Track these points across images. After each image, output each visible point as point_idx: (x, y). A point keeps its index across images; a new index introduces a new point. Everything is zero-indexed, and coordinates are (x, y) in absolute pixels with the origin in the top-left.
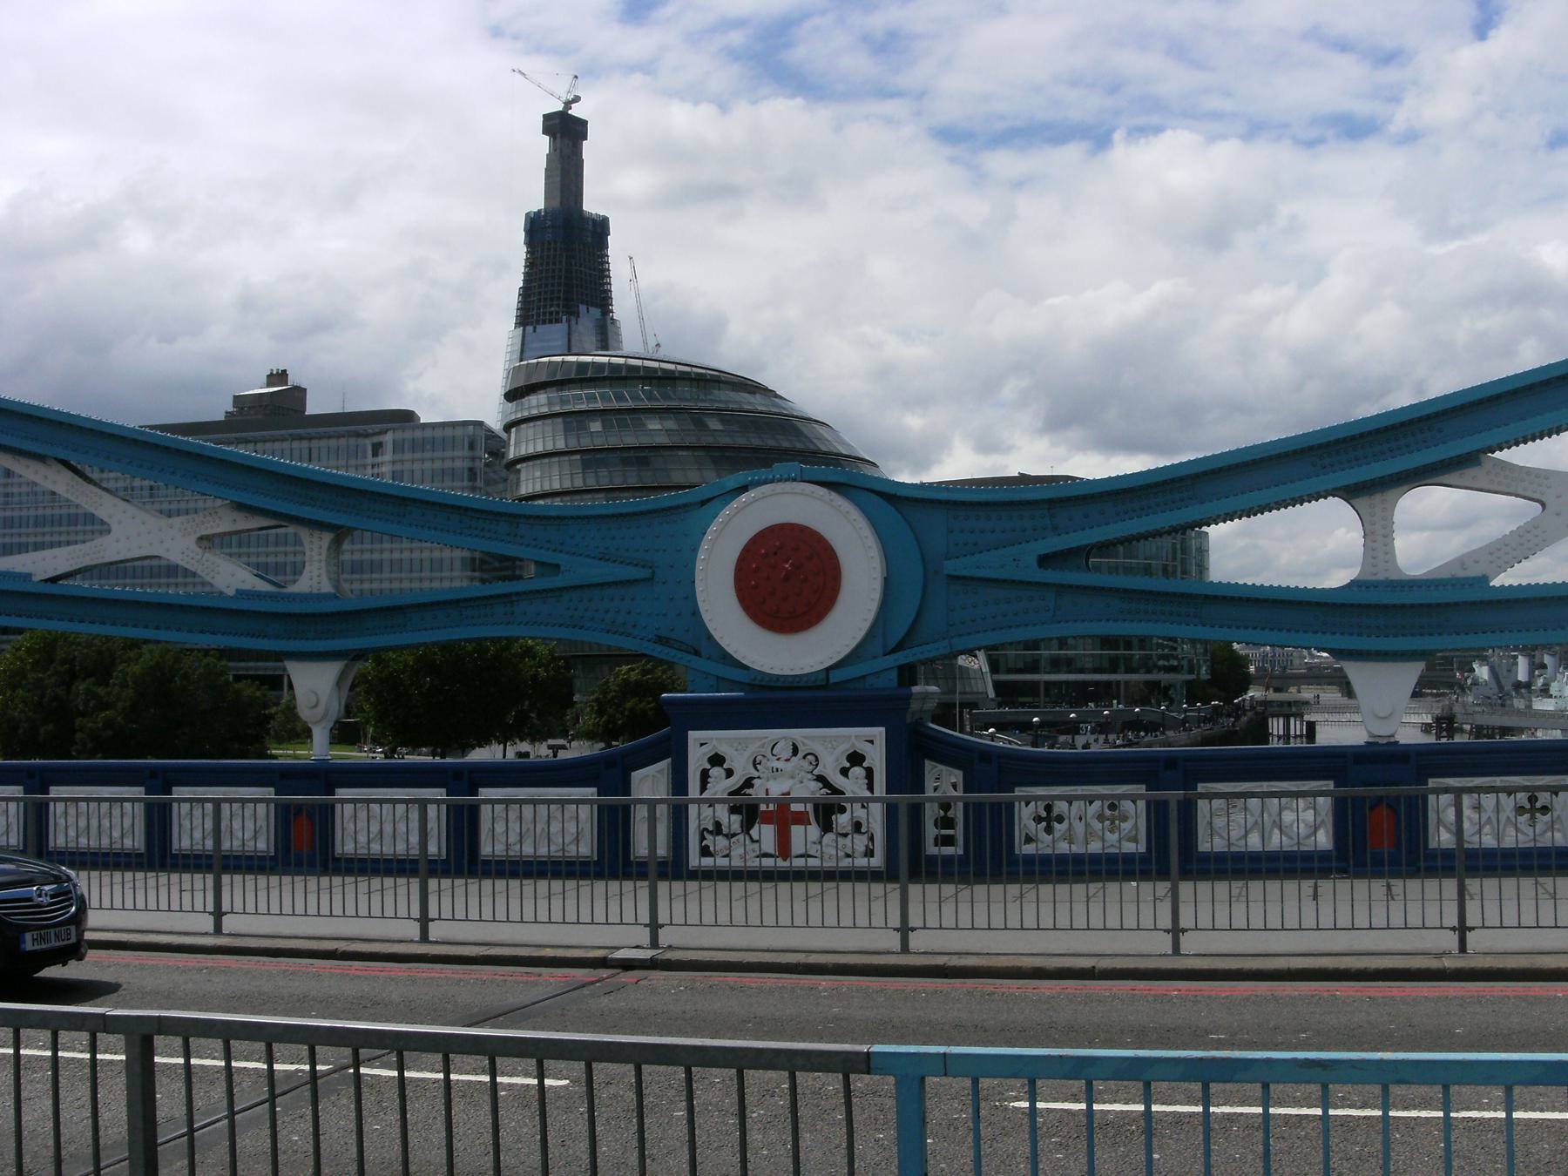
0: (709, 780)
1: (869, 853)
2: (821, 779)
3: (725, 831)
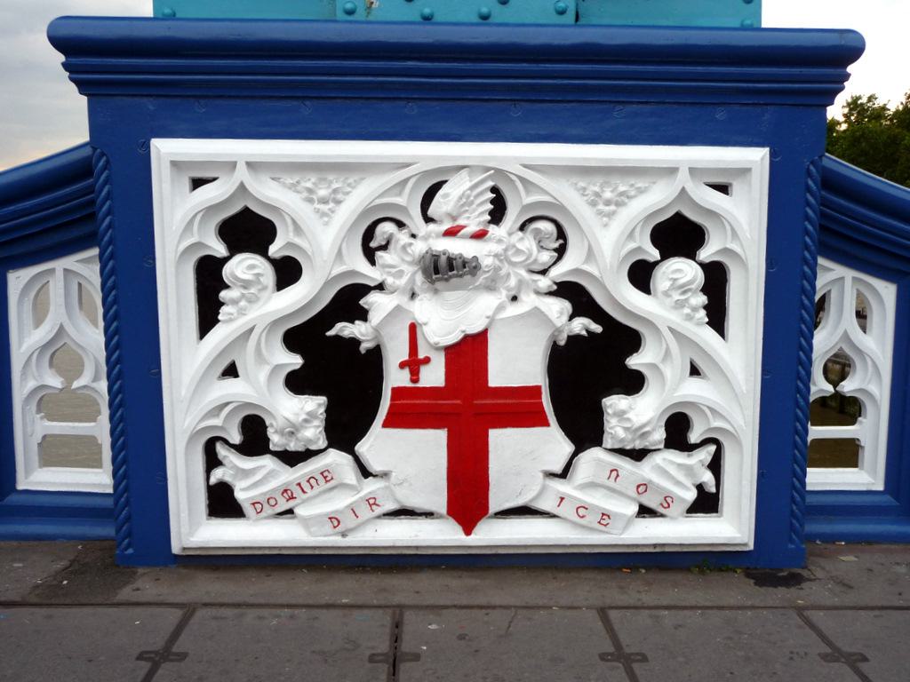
0: (224, 295)
2: (575, 295)
3: (276, 440)
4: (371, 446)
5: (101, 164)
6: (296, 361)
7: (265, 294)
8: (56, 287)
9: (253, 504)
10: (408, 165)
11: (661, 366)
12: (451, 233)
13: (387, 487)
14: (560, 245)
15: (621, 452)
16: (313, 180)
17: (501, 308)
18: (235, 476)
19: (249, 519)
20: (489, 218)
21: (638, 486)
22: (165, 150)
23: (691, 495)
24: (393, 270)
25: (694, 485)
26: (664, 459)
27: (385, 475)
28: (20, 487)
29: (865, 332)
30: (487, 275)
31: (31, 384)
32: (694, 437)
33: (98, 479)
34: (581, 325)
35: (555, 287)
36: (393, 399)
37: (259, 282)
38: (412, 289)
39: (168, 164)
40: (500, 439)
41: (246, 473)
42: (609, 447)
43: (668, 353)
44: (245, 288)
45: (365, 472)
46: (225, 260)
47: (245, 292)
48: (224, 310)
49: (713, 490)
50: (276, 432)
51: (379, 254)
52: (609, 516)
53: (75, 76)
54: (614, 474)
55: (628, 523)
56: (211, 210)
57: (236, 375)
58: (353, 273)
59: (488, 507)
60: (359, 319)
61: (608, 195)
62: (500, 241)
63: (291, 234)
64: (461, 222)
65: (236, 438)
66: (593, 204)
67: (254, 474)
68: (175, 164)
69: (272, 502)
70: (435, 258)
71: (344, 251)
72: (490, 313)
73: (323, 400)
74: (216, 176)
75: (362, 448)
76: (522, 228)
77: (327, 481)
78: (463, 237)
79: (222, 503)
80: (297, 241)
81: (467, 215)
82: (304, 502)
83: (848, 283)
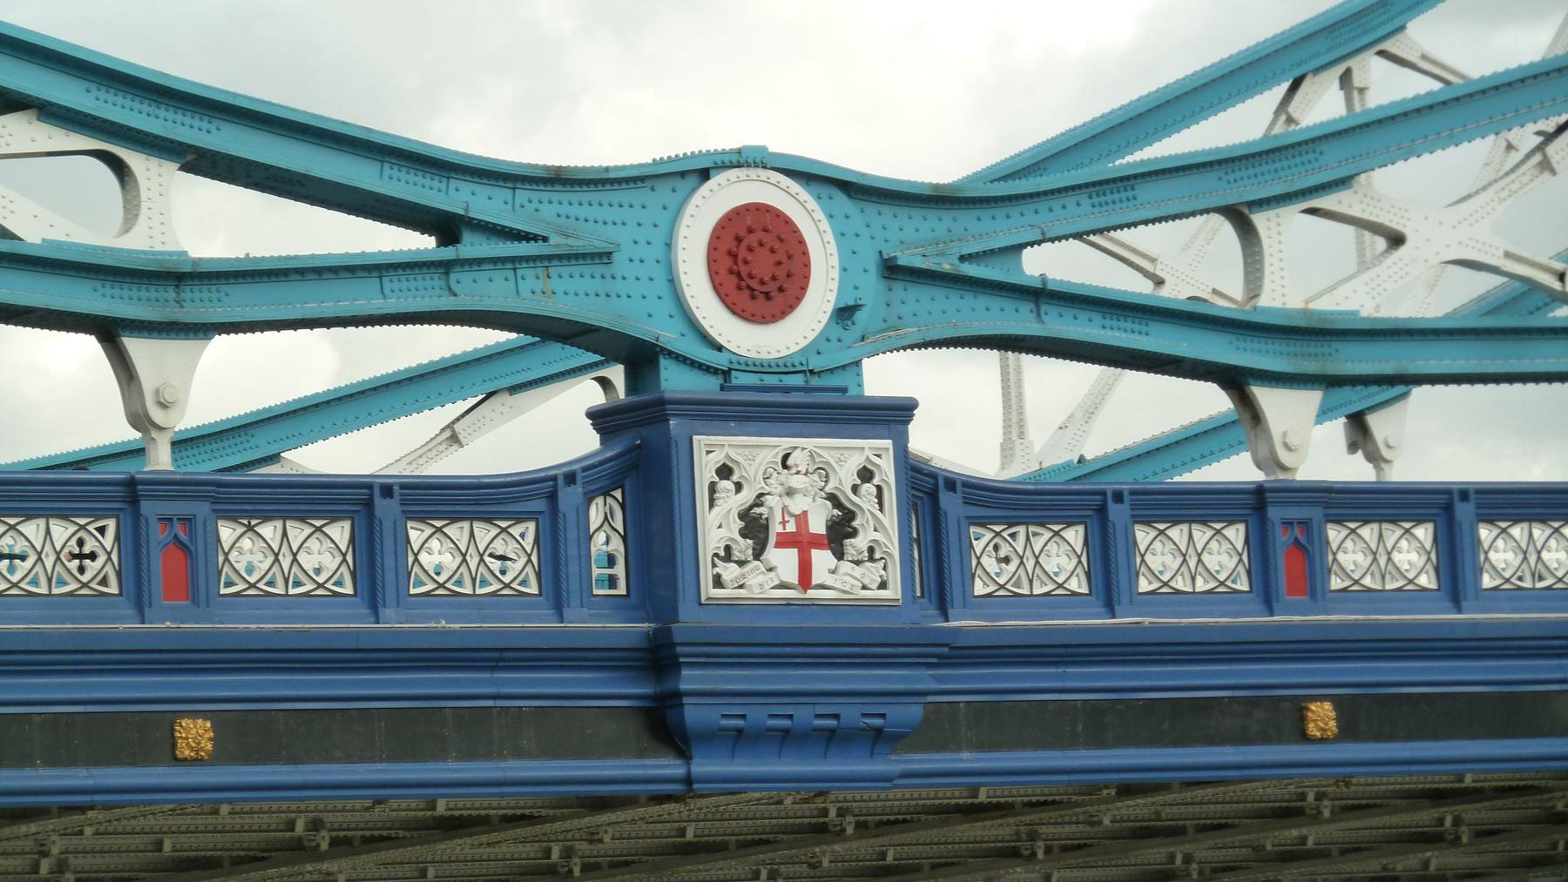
0: (717, 495)
1: (883, 585)
32: (877, 556)
43: (868, 519)
79: (718, 582)
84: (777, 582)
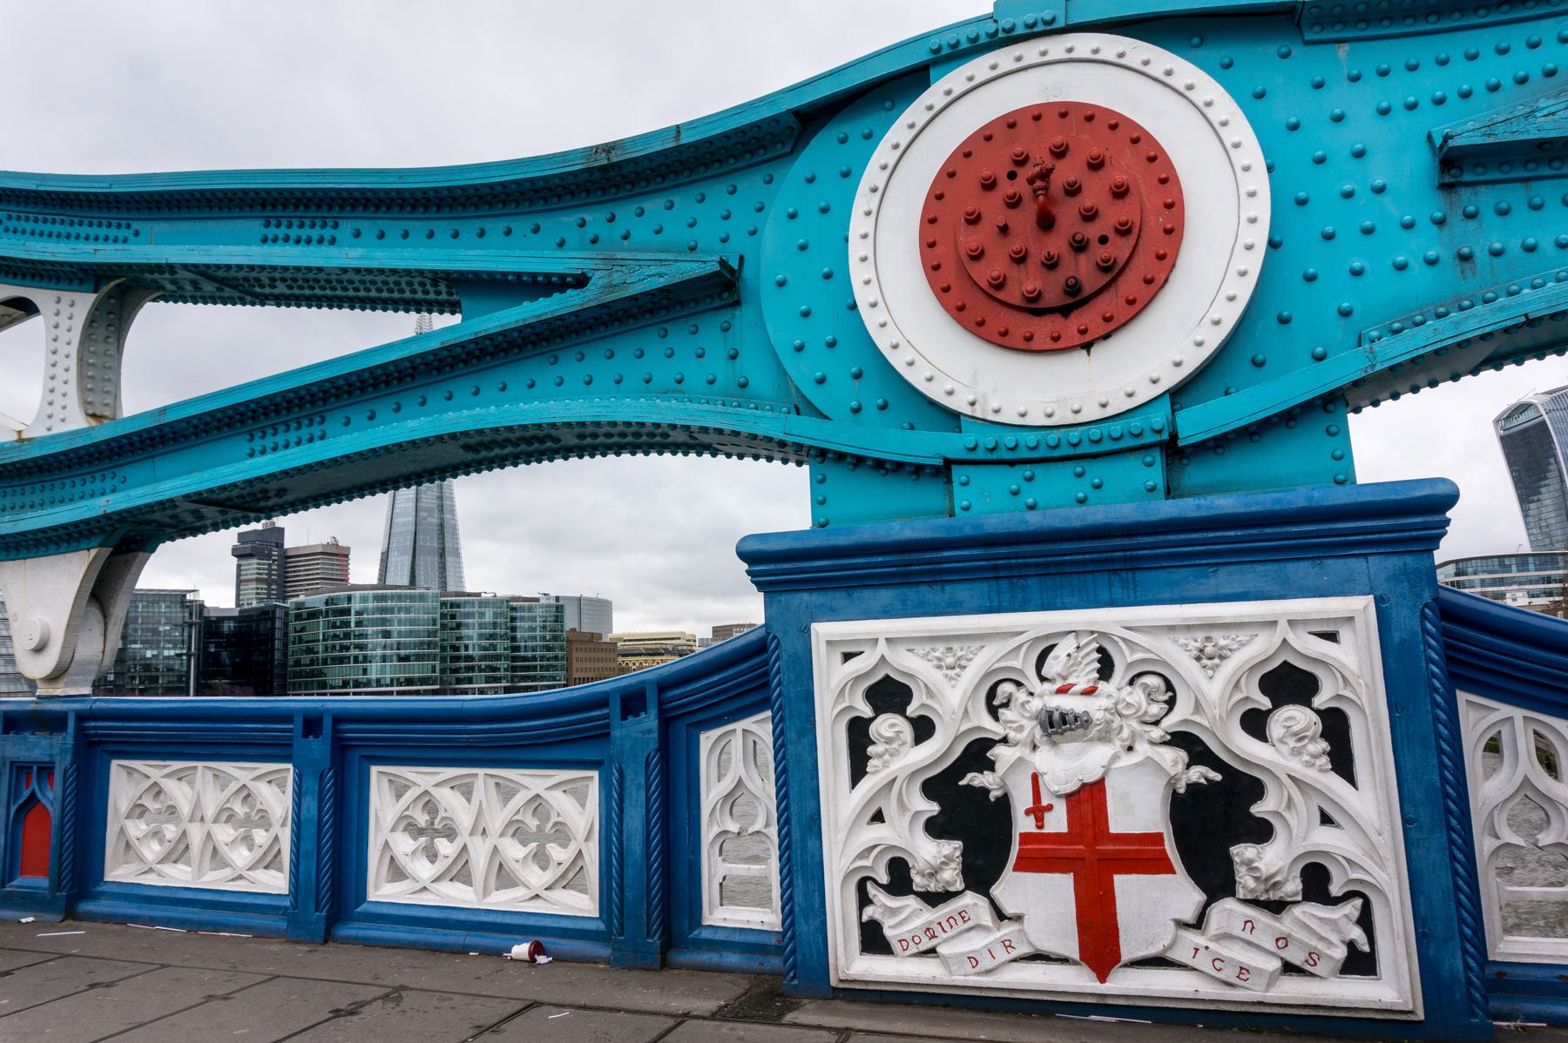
0: (871, 750)
3: (919, 882)
4: (1004, 889)
5: (773, 645)
6: (934, 808)
7: (903, 749)
8: (737, 743)
9: (900, 941)
10: (1022, 633)
11: (1284, 814)
12: (1063, 691)
13: (1020, 931)
14: (1170, 697)
15: (1254, 903)
16: (941, 650)
17: (1115, 758)
18: (883, 914)
19: (897, 956)
20: (1098, 675)
21: (1277, 940)
22: (823, 631)
23: (1340, 953)
24: (1014, 725)
25: (1343, 942)
26: (1304, 912)
27: (1018, 918)
28: (706, 922)
29: (1556, 778)
30: (1099, 728)
31: (716, 830)
32: (1335, 889)
33: (766, 918)
34: (1198, 773)
35: (1169, 737)
36: (1020, 844)
37: (900, 739)
38: (1033, 742)
39: (825, 644)
40: (1127, 887)
41: (894, 912)
42: (1241, 897)
43: (1290, 799)
44: (887, 743)
45: (1000, 915)
46: (872, 720)
47: (887, 747)
48: (871, 763)
49: (1366, 949)
50: (918, 873)
51: (1001, 711)
52: (1248, 971)
53: (755, 579)
54: (1249, 925)
55: (1272, 980)
56: (859, 678)
57: (883, 821)
58: (979, 729)
59: (1120, 957)
60: (987, 770)
61: (1209, 649)
62: (1109, 696)
63: (924, 697)
64: (1070, 681)
65: (884, 878)
66: (1198, 659)
67: (901, 913)
68: (829, 643)
69: (917, 940)
70: (1050, 714)
71: (970, 710)
72: (1105, 763)
73: (958, 844)
74: (861, 650)
75: (997, 891)
76: (1131, 683)
77: (965, 922)
78: (1073, 694)
79: (873, 940)
80: (930, 702)
81: (1076, 674)
82: (946, 941)
83: (1519, 723)
84: (1024, 950)
